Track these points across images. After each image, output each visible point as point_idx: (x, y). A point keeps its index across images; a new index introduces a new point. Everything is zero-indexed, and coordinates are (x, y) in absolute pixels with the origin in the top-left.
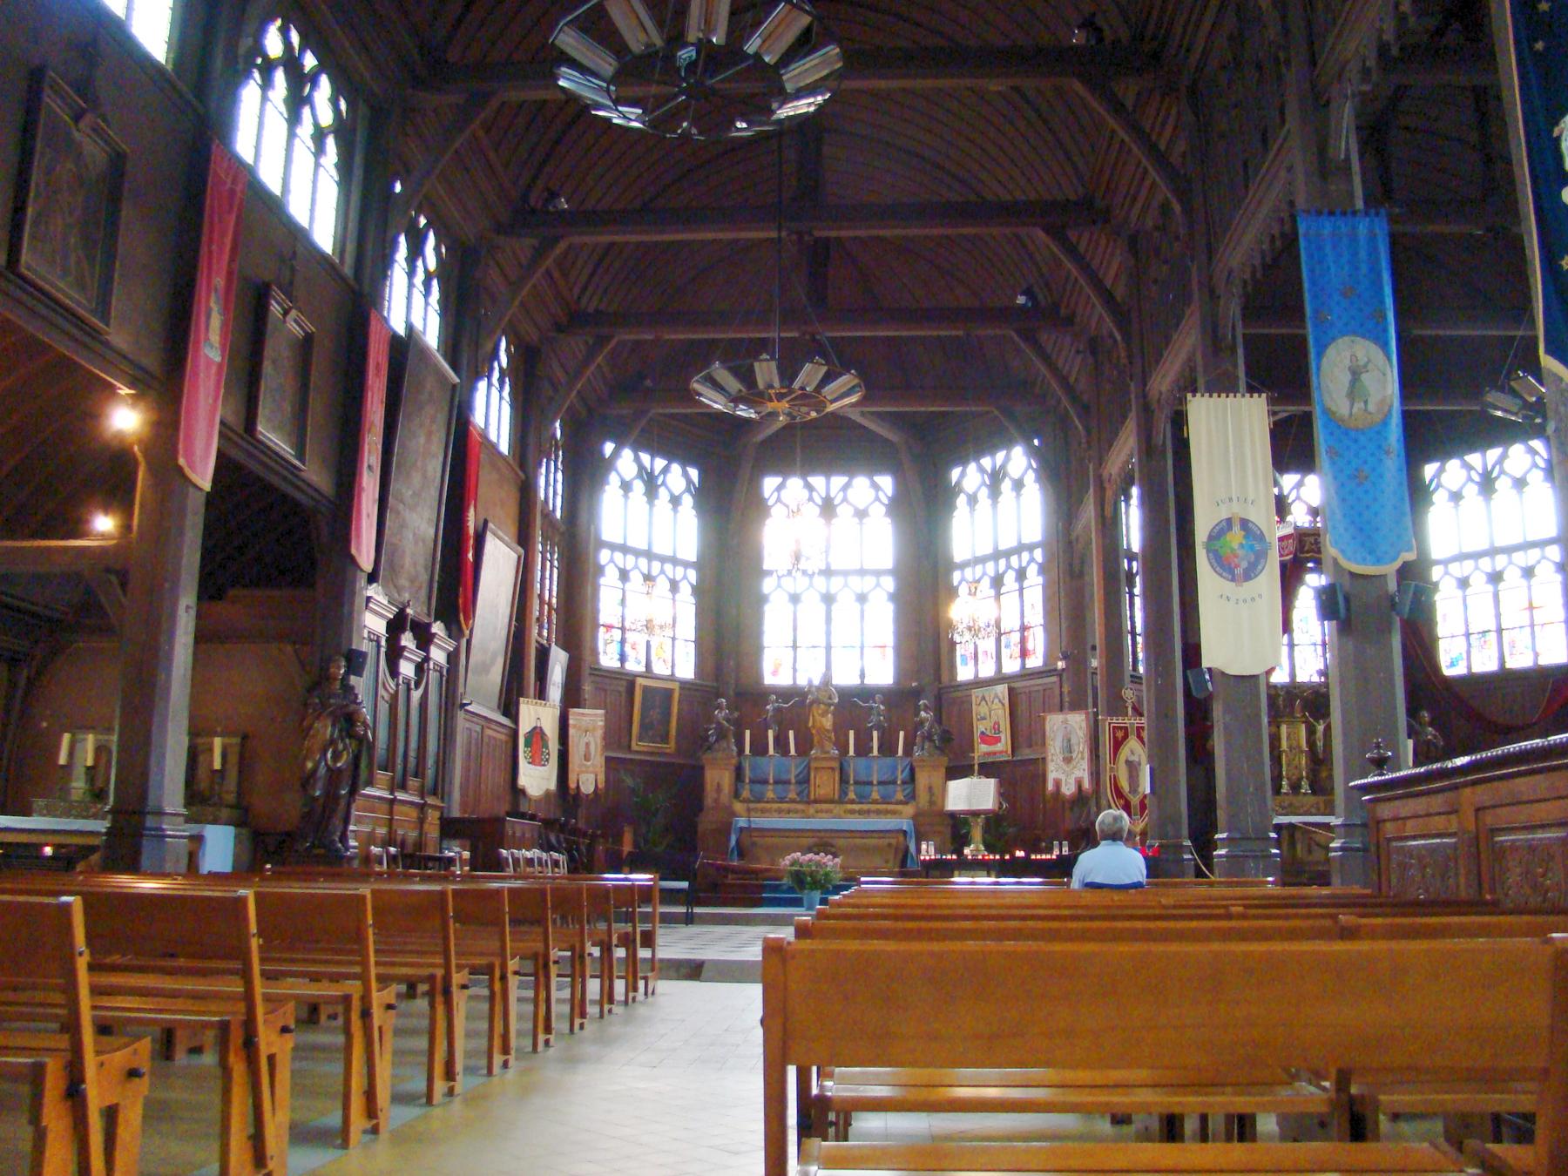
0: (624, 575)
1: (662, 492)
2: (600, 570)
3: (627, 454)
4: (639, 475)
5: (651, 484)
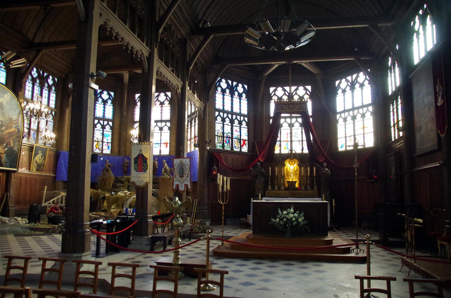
0: (223, 120)
4: (227, 87)
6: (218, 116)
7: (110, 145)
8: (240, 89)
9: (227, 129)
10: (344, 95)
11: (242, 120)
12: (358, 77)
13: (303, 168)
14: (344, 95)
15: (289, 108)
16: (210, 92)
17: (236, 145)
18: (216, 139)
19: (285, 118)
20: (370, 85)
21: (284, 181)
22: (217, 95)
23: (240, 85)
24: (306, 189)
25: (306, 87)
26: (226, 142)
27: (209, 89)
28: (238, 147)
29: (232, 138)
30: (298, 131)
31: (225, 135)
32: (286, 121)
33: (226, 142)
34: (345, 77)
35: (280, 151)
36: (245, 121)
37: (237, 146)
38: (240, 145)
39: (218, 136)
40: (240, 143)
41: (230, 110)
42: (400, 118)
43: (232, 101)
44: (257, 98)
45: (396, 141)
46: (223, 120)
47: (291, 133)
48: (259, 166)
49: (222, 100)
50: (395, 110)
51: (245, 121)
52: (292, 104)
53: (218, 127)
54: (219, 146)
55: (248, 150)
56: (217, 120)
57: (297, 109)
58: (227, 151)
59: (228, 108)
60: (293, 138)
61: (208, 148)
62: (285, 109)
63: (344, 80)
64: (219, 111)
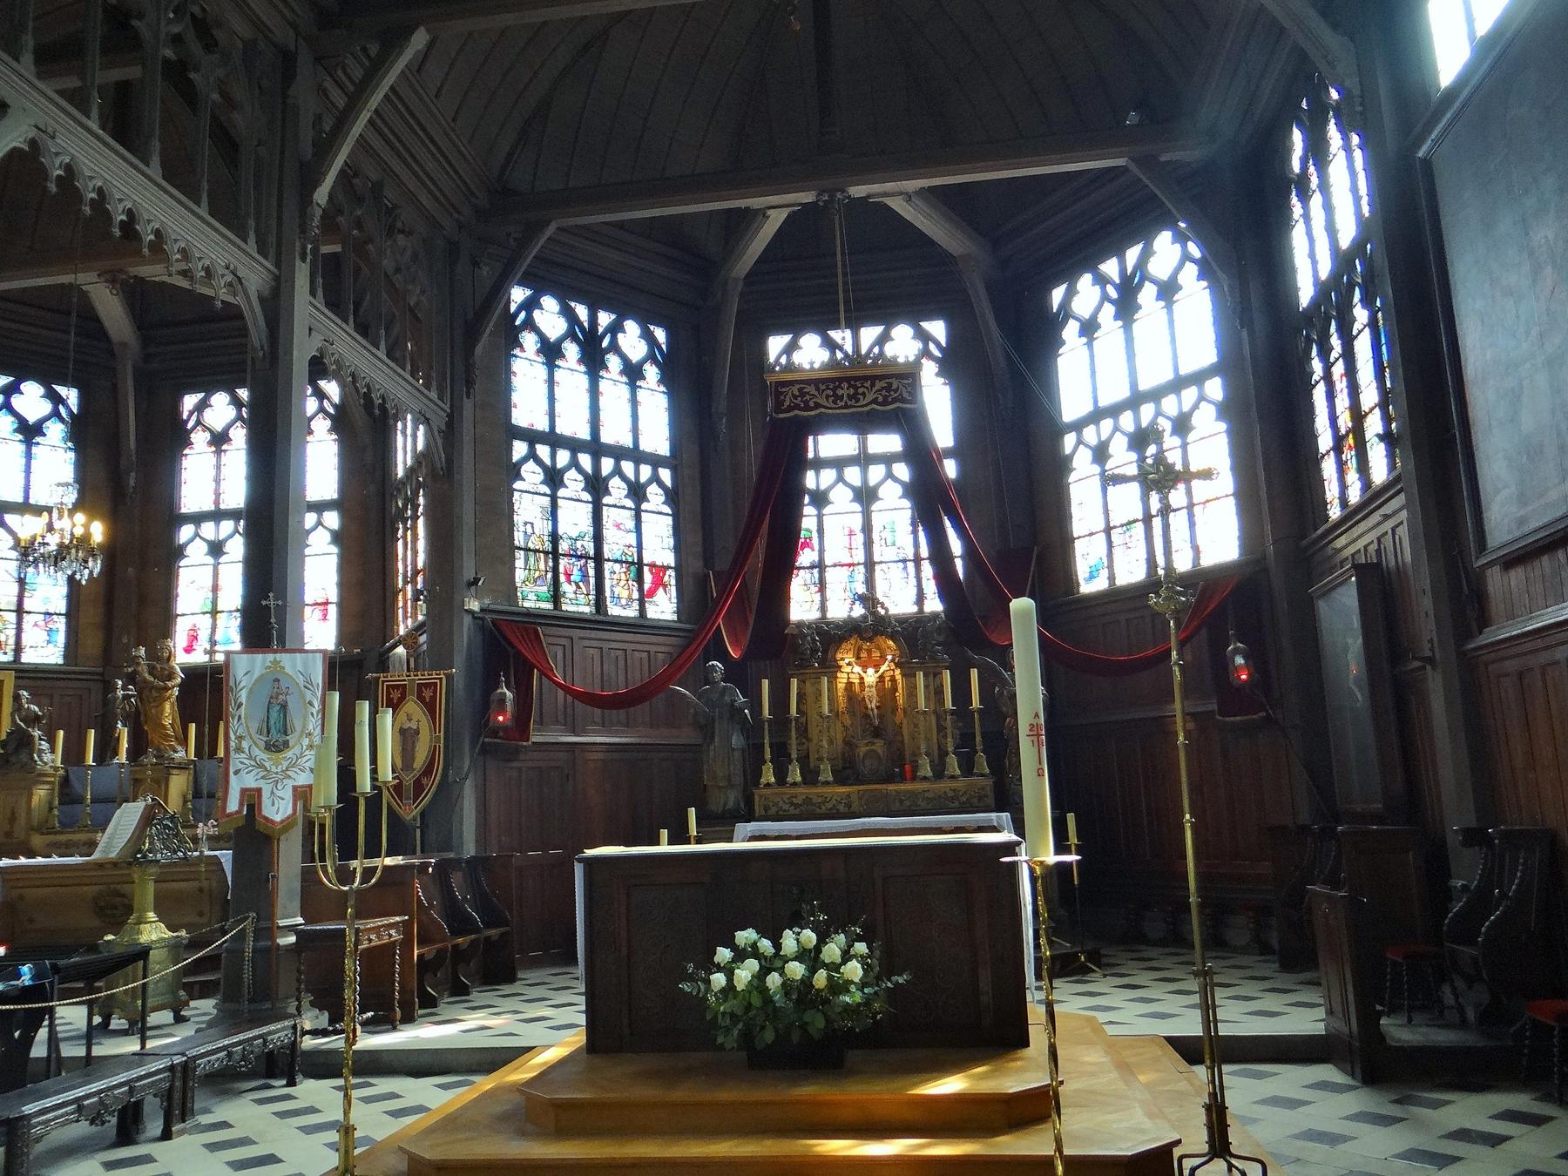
0: (554, 478)
2: (515, 472)
3: (549, 303)
4: (570, 335)
6: (525, 460)
7: (61, 624)
8: (632, 341)
9: (575, 519)
10: (1090, 345)
11: (643, 479)
12: (1146, 254)
13: (920, 675)
14: (1090, 345)
15: (838, 398)
16: (479, 350)
17: (617, 590)
18: (519, 563)
19: (839, 464)
20: (1205, 284)
22: (518, 365)
23: (632, 327)
24: (939, 772)
25: (925, 325)
26: (568, 576)
27: (472, 333)
28: (630, 598)
29: (599, 558)
30: (895, 512)
31: (564, 546)
32: (840, 479)
33: (568, 576)
34: (1090, 263)
35: (823, 608)
36: (661, 484)
37: (625, 594)
38: (641, 589)
39: (527, 550)
40: (639, 579)
41: (584, 434)
42: (1370, 396)
43: (594, 393)
45: (1353, 515)
46: (554, 478)
47: (867, 529)
48: (718, 676)
49: (544, 388)
50: (1338, 369)
51: (661, 484)
52: (848, 379)
53: (528, 509)
54: (533, 597)
55: (678, 612)
56: (518, 476)
57: (875, 401)
58: (577, 621)
59: (573, 424)
60: (876, 548)
61: (474, 605)
62: (818, 406)
63: (1086, 280)
64: (532, 437)
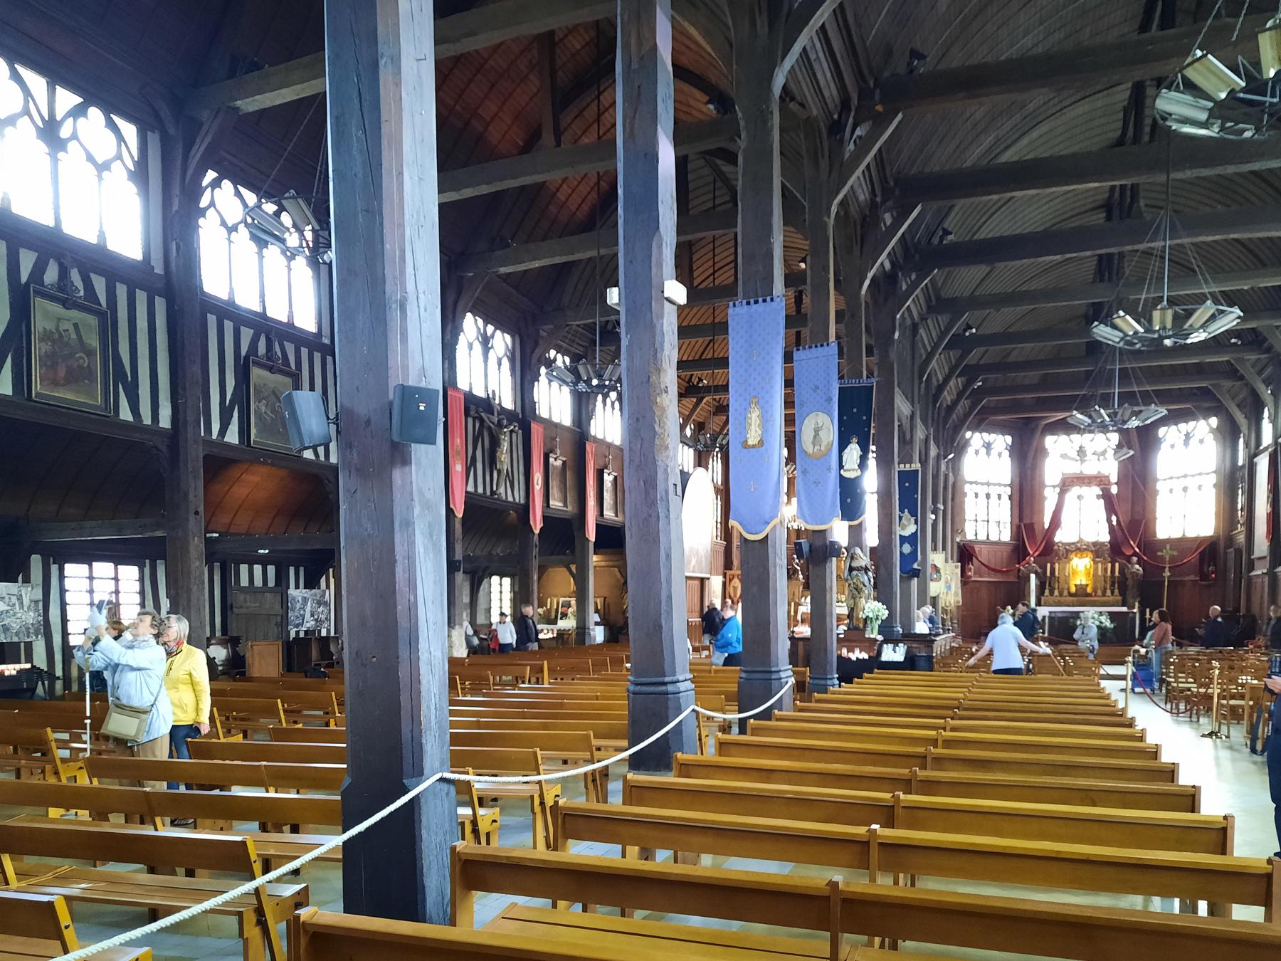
1: (994, 453)
5: (988, 446)
21: (1068, 583)
44: (1026, 458)
